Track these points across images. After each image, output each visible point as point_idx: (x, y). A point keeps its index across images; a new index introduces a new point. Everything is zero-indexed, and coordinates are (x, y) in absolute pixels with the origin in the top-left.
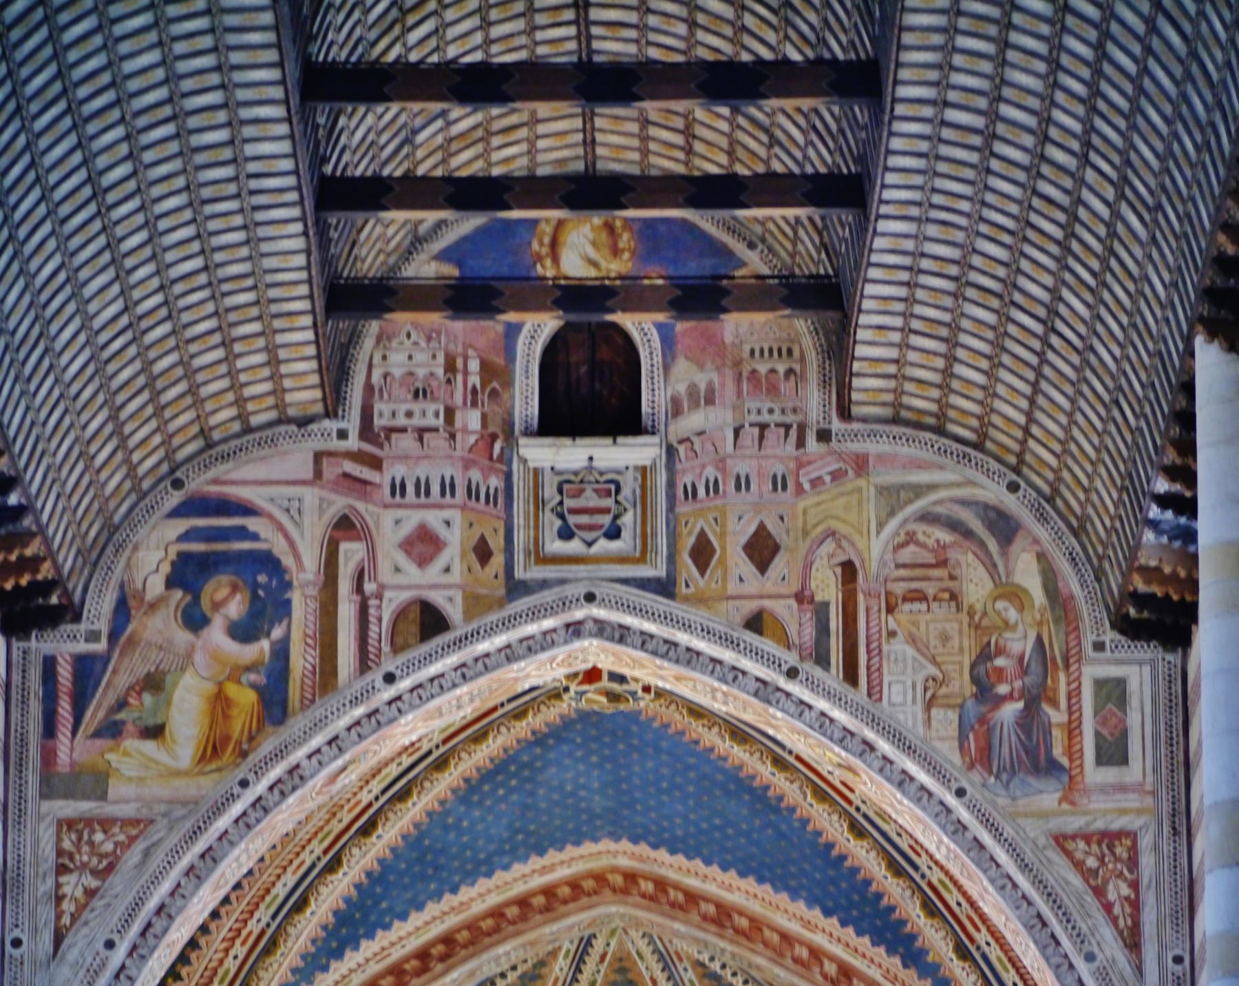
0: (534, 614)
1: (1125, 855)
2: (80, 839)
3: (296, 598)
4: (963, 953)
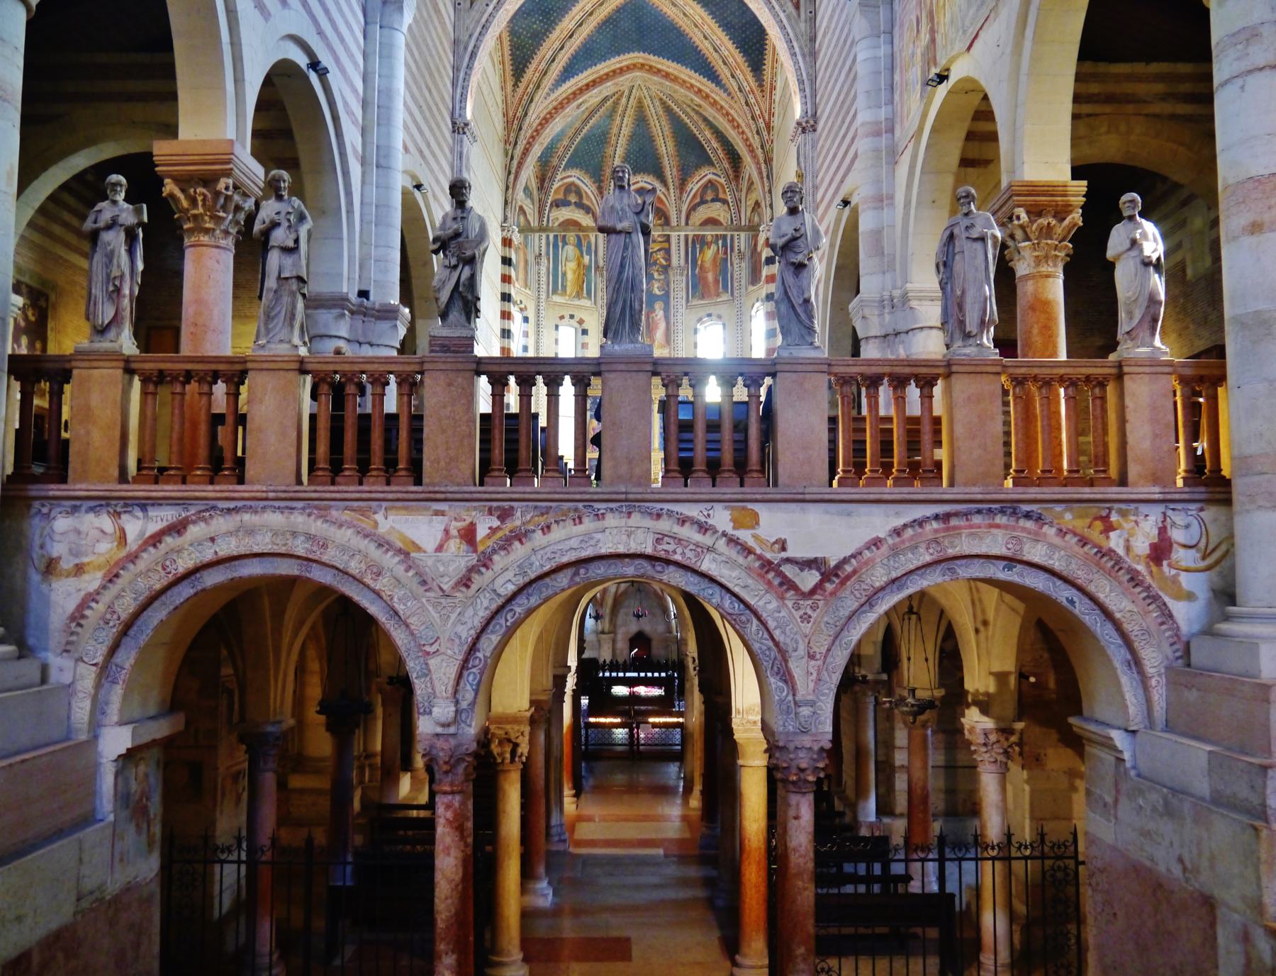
4: (733, 76)
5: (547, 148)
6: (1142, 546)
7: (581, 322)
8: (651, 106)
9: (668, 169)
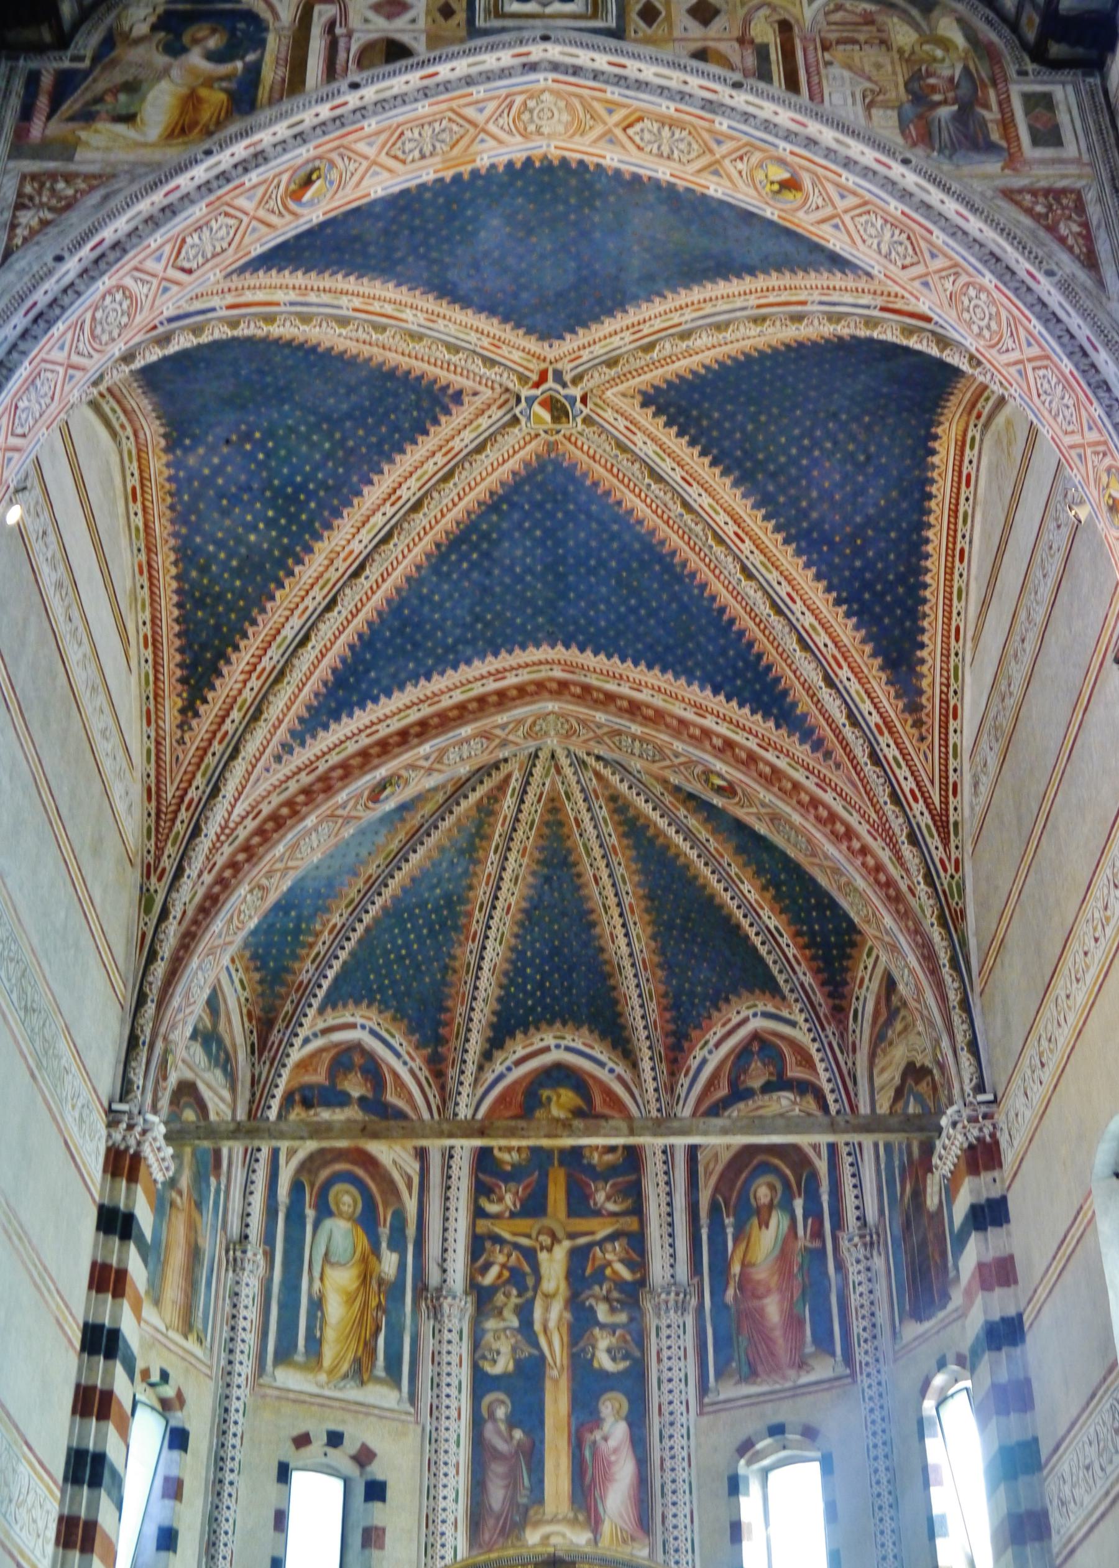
0: (493, 48)
1: (1071, 204)
2: (42, 185)
3: (272, 41)
4: (829, 682)
5: (282, 907)
8: (586, 817)
9: (636, 1001)
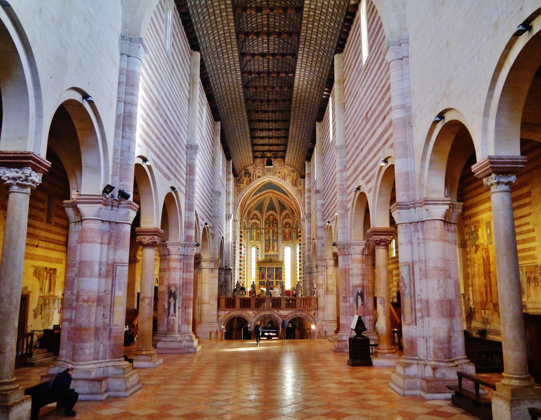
6: (313, 314)
7: (257, 246)
